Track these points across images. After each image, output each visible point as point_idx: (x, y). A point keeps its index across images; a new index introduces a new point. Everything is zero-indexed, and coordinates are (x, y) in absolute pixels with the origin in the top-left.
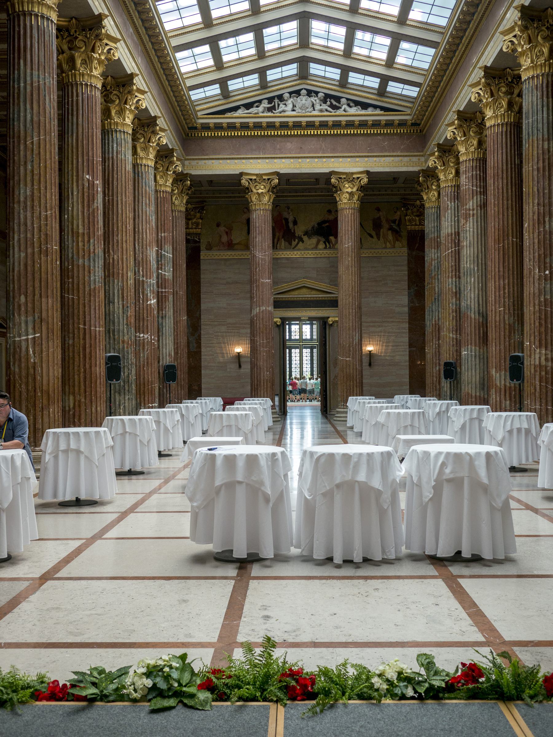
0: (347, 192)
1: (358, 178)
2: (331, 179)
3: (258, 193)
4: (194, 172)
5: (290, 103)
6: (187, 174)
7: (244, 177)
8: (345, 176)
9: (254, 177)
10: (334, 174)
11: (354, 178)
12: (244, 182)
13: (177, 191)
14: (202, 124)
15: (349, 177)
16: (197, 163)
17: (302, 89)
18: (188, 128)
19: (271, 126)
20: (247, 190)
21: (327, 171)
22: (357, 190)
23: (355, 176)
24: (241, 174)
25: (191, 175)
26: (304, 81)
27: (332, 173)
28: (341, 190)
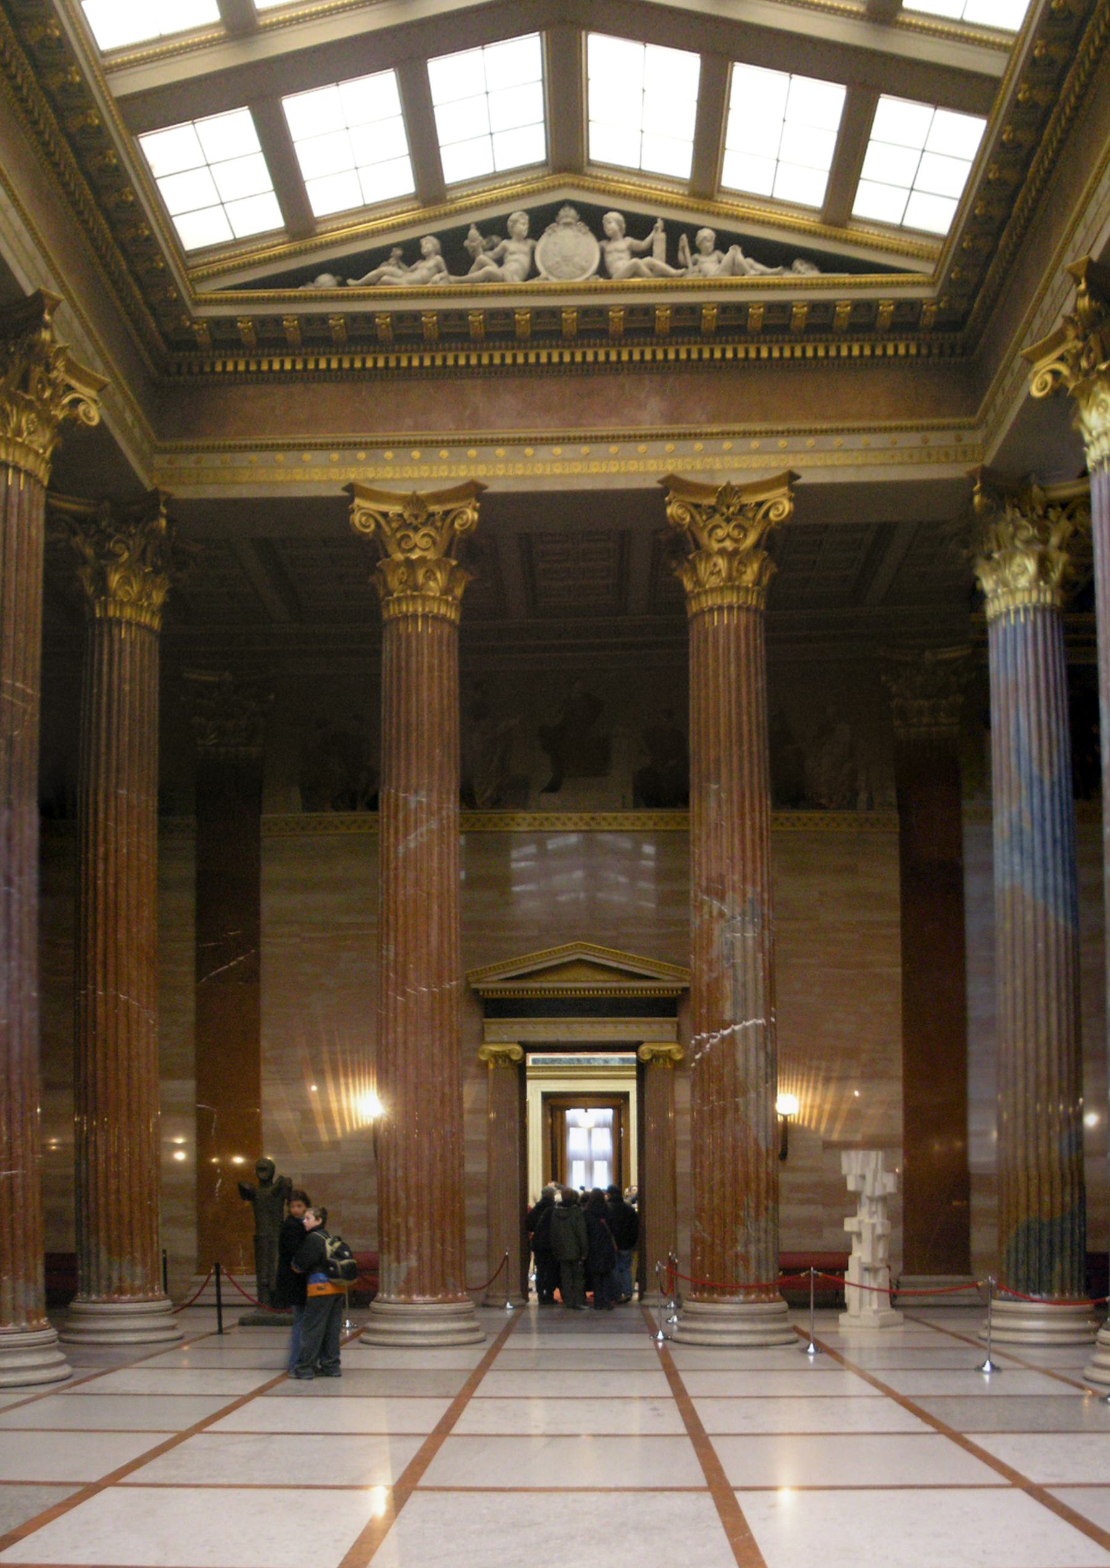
0: (722, 552)
1: (759, 505)
2: (665, 505)
3: (408, 560)
4: (181, 493)
5: (517, 253)
6: (156, 493)
7: (358, 501)
8: (712, 501)
10: (676, 490)
11: (743, 508)
13: (126, 555)
14: (217, 323)
16: (198, 462)
17: (562, 204)
18: (165, 335)
21: (652, 484)
22: (756, 546)
23: (751, 500)
24: (352, 489)
25: (170, 502)
26: (568, 178)
27: (672, 484)
28: (698, 546)
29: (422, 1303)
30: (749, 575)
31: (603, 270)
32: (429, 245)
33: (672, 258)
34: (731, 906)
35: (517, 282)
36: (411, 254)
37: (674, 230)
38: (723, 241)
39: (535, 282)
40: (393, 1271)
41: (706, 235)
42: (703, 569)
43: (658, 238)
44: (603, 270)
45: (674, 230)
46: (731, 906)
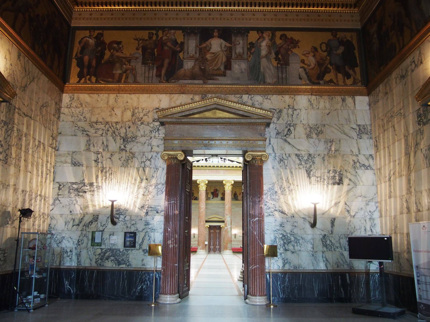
9: (200, 181)
12: (198, 182)
15: (228, 181)
19: (206, 166)
20: (199, 184)
24: (197, 180)
29: (201, 250)
30: (230, 187)
31: (218, 162)
32: (204, 160)
33: (224, 162)
34: (228, 216)
35: (211, 163)
36: (203, 160)
37: (224, 159)
38: (229, 160)
39: (213, 163)
40: (199, 248)
41: (227, 160)
42: (226, 187)
43: (223, 159)
44: (218, 162)
45: (224, 159)
46: (228, 216)
